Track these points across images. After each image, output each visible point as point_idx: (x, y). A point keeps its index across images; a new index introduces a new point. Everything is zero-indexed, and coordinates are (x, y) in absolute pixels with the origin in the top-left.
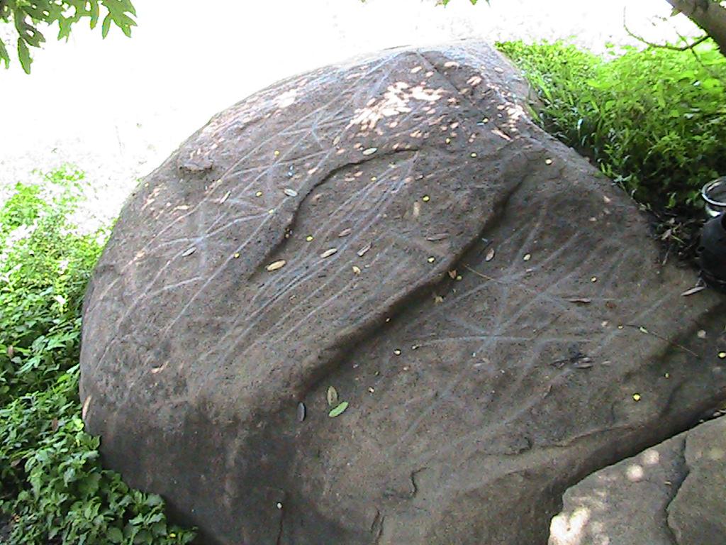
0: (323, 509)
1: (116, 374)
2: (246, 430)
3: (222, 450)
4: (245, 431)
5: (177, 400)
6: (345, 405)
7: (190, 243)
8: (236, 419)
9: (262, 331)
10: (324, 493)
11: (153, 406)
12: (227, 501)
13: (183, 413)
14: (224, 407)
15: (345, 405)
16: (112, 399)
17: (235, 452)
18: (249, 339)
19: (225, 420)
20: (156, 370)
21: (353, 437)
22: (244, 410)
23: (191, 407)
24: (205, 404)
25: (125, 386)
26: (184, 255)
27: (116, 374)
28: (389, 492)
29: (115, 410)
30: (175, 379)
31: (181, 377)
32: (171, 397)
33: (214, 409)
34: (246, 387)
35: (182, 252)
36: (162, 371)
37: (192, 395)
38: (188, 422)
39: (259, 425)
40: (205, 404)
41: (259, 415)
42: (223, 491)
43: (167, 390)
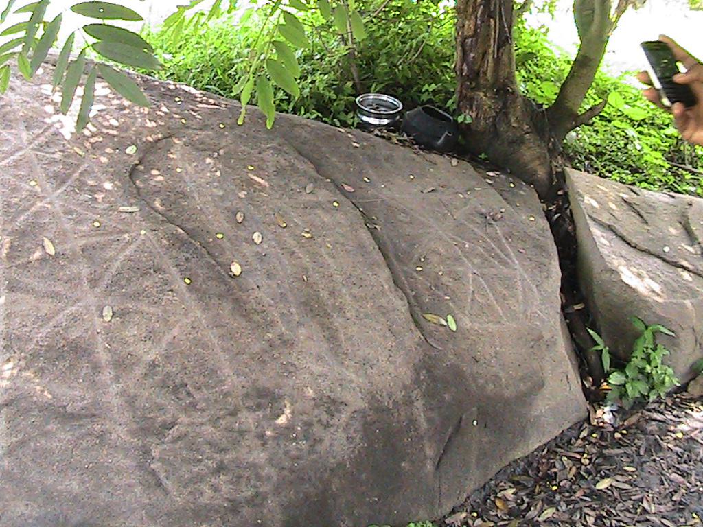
0: (507, 393)
1: (221, 469)
2: (415, 389)
3: (412, 421)
4: (416, 392)
5: (344, 417)
6: (450, 318)
7: (87, 308)
8: (405, 387)
9: (329, 316)
10: (503, 380)
11: (319, 448)
12: (429, 466)
13: (357, 425)
14: (392, 384)
15: (450, 318)
16: (249, 492)
17: (422, 415)
18: (322, 325)
19: (400, 395)
20: (282, 420)
21: (480, 331)
22: (406, 374)
23: (363, 412)
24: (373, 397)
25: (254, 466)
26: (108, 319)
27: (221, 469)
28: (532, 343)
29: (265, 498)
30: (316, 406)
31: (321, 399)
32: (331, 422)
33: (384, 394)
34: (390, 356)
35: (97, 320)
36: (292, 413)
37: (357, 402)
38: (367, 427)
39: (422, 377)
40: (373, 397)
41: (417, 371)
42: (426, 457)
43: (319, 421)
